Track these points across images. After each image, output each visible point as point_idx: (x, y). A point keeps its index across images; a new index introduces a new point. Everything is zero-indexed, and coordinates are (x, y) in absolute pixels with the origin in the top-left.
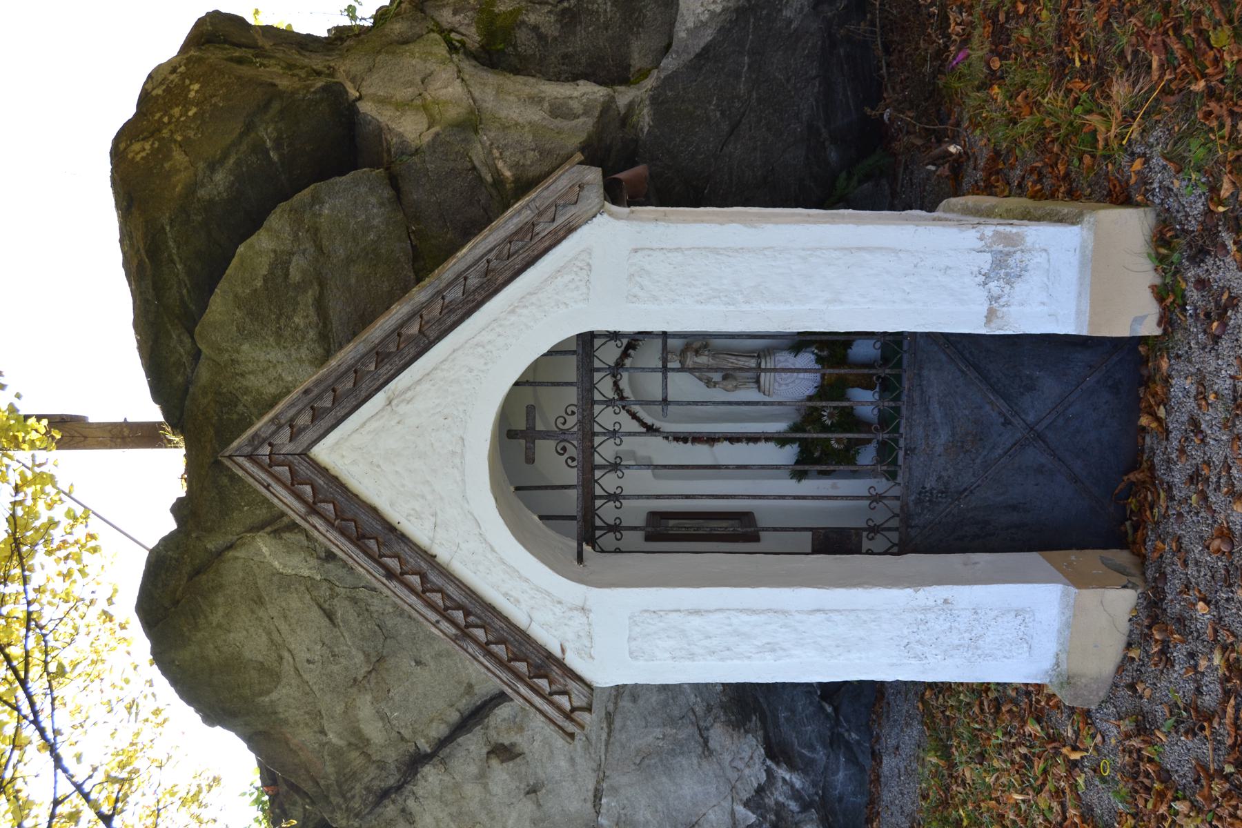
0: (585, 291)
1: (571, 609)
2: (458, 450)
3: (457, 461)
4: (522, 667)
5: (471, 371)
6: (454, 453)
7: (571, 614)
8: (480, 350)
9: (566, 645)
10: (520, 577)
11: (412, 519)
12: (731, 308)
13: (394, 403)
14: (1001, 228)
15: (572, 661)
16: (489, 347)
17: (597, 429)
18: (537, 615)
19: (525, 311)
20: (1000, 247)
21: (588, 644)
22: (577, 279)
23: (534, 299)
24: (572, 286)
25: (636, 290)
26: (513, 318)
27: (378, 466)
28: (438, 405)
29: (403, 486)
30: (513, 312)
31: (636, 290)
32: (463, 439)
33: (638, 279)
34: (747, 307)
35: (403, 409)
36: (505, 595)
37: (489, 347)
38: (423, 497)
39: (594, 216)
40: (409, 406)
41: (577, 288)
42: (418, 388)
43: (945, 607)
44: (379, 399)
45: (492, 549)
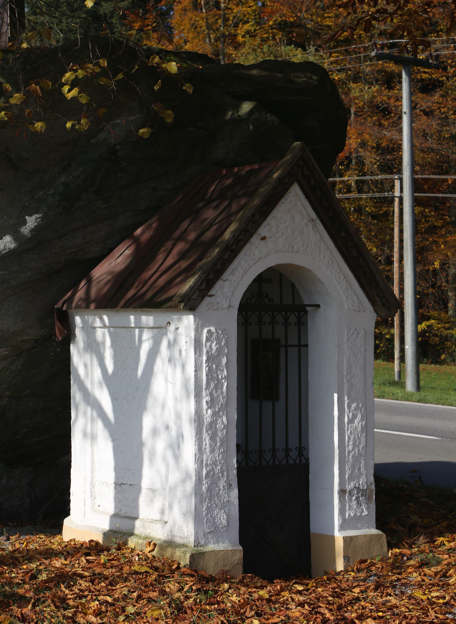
0: (352, 309)
1: (230, 301)
2: (294, 250)
3: (291, 249)
4: (211, 276)
5: (324, 257)
6: (293, 248)
7: (228, 300)
8: (331, 262)
9: (214, 298)
10: (243, 276)
11: (269, 227)
12: (345, 373)
13: (312, 222)
14: (374, 491)
15: (207, 300)
16: (332, 266)
17: (276, 313)
18: (227, 284)
19: (345, 282)
20: (368, 493)
21: (214, 309)
22: (356, 305)
23: (349, 286)
24: (353, 303)
25: (352, 332)
26: (342, 277)
27: (289, 213)
28: (311, 242)
29: (281, 223)
30: (345, 277)
31: (352, 332)
32: (298, 252)
33: (356, 333)
34: (345, 381)
35: (310, 226)
36: (236, 268)
37: (332, 266)
38: (277, 233)
39: (376, 314)
40: (311, 229)
41: (353, 306)
42: (318, 234)
43: (229, 485)
44: (313, 215)
45: (255, 263)
